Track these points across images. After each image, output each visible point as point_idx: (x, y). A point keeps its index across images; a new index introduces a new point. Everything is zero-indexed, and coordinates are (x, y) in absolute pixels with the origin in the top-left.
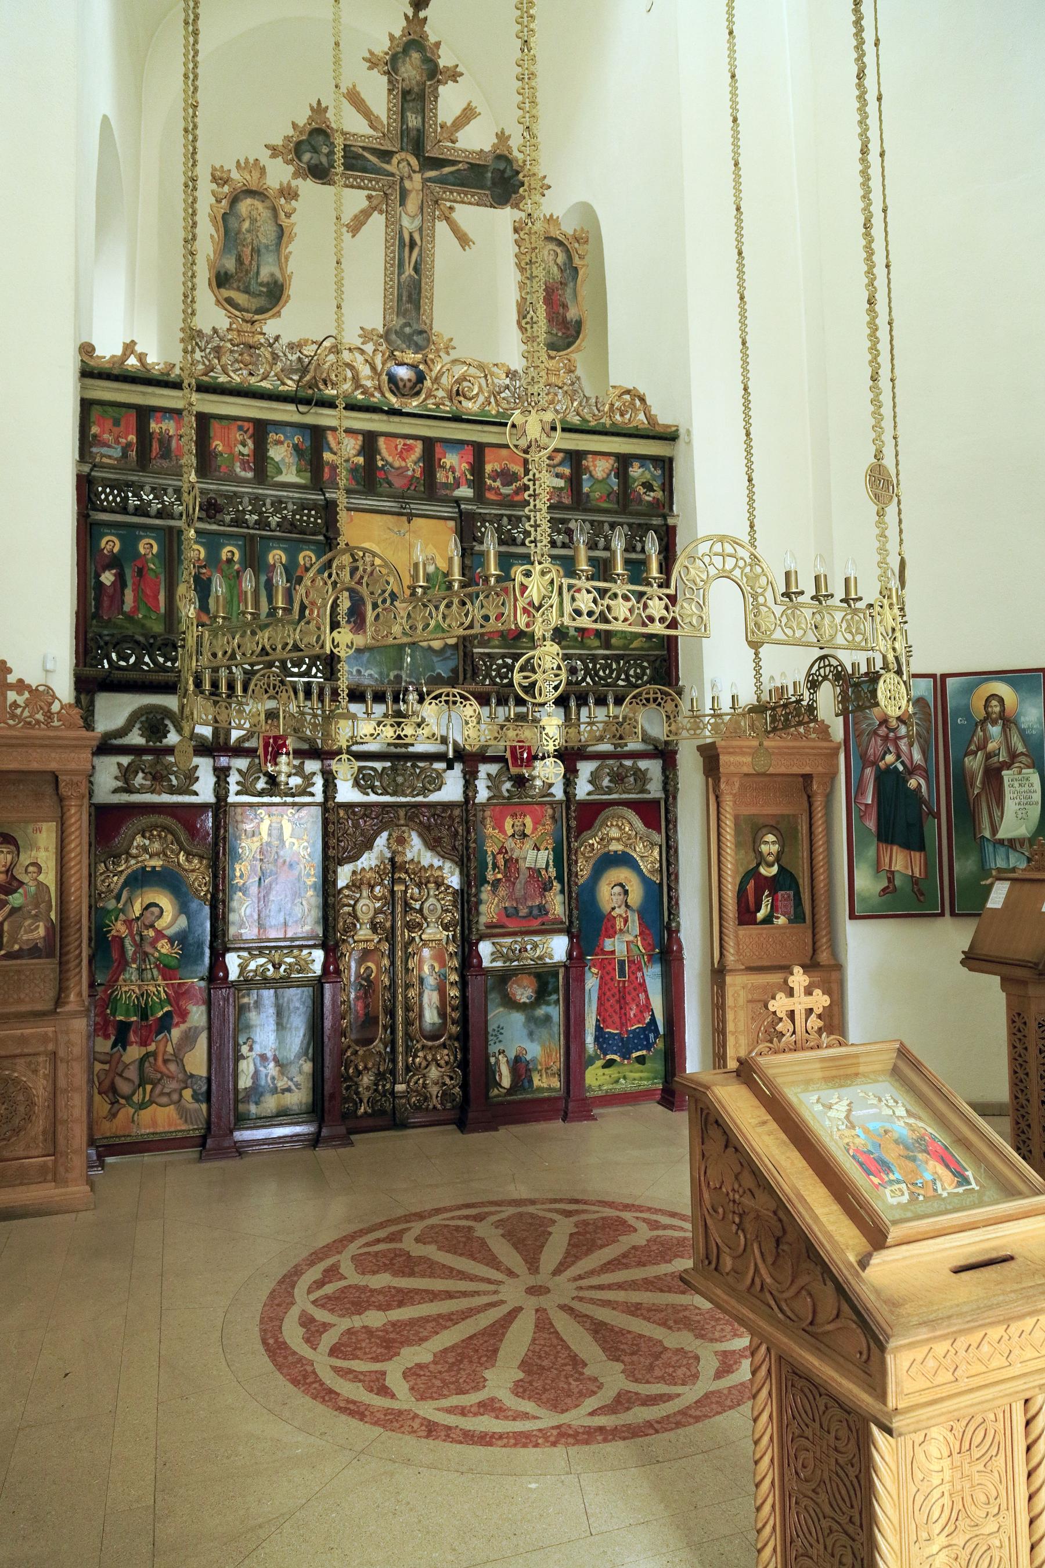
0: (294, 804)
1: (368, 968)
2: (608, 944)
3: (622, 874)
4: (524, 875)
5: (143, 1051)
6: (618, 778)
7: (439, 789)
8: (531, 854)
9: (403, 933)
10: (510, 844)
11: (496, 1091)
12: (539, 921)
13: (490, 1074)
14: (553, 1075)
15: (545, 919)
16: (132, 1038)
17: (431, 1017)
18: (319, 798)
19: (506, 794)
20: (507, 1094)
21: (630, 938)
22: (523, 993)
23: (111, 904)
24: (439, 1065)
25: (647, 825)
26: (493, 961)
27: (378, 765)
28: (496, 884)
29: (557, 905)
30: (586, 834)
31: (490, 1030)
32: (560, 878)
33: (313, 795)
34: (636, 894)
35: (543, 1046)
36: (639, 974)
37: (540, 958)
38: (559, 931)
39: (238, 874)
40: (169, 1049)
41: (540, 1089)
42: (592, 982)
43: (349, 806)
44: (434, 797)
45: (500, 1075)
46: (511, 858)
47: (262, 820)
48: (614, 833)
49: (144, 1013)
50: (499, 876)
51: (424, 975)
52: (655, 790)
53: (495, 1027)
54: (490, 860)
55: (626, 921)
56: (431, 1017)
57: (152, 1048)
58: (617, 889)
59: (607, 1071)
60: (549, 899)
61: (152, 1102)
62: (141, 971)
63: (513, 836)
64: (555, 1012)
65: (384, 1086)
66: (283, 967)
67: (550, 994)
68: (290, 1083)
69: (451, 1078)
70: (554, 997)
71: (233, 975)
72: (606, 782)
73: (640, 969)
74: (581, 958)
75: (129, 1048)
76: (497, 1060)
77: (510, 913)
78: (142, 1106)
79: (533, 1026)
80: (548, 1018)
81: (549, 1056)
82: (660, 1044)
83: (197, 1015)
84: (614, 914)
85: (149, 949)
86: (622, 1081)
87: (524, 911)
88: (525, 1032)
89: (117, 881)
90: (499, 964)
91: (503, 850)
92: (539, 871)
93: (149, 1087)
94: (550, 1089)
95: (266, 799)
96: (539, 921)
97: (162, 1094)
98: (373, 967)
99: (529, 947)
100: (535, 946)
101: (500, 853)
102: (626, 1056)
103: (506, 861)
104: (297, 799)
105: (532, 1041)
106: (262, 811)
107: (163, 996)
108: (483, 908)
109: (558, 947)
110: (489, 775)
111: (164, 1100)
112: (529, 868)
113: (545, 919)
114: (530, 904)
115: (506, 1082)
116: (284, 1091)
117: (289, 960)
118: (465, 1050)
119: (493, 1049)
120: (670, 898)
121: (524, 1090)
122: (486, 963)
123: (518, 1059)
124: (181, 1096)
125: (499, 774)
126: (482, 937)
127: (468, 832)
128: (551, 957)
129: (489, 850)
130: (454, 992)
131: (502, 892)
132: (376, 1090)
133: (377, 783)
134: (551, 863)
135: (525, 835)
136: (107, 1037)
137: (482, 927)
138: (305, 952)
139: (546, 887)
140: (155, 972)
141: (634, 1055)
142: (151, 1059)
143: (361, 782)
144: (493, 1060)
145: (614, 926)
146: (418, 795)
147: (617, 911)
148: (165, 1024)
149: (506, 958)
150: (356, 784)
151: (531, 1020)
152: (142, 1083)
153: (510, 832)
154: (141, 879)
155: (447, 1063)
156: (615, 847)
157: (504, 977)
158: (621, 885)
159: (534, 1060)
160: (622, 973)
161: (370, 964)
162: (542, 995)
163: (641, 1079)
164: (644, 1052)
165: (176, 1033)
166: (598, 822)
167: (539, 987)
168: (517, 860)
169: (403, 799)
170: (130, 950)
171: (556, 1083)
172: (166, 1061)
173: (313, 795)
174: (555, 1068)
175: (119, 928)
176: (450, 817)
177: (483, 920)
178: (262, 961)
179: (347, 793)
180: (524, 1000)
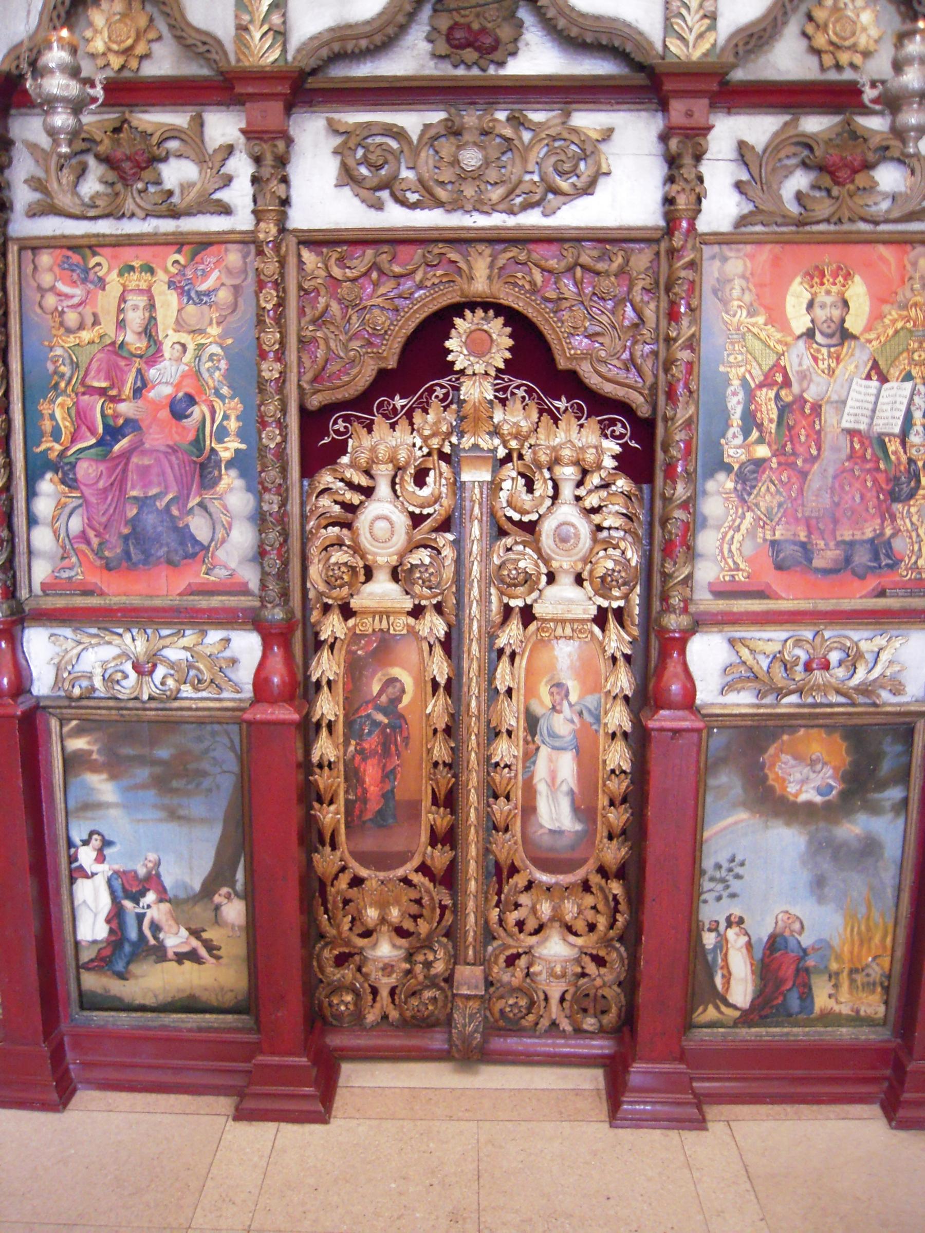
0: (178, 242)
1: (393, 681)
4: (834, 453)
7: (588, 189)
8: (862, 391)
9: (485, 599)
10: (797, 358)
11: (711, 1013)
12: (872, 583)
13: (696, 975)
14: (870, 987)
15: (888, 580)
17: (555, 814)
18: (243, 220)
19: (793, 208)
20: (736, 1023)
22: (807, 777)
24: (570, 929)
26: (727, 688)
27: (412, 121)
28: (749, 475)
31: (708, 863)
33: (225, 210)
35: (851, 917)
37: (865, 689)
39: (47, 425)
41: (828, 1018)
43: (318, 241)
44: (575, 215)
45: (727, 978)
46: (801, 400)
47: (102, 283)
50: (762, 451)
51: (538, 709)
53: (723, 858)
54: (735, 405)
56: (555, 814)
63: (810, 334)
65: (428, 965)
66: (160, 671)
67: (882, 786)
68: (195, 943)
69: (600, 961)
70: (895, 794)
76: (722, 944)
77: (789, 559)
79: (826, 866)
80: (870, 848)
81: (865, 940)
87: (826, 555)
88: (804, 877)
90: (743, 700)
91: (777, 377)
92: (881, 441)
94: (857, 1020)
95: (105, 227)
96: (872, 583)
98: (407, 680)
99: (834, 657)
100: (852, 659)
101: (767, 382)
103: (784, 410)
104: (189, 225)
105: (821, 900)
106: (101, 262)
108: (707, 541)
110: (742, 147)
112: (852, 433)
113: (888, 580)
114: (846, 534)
115: (741, 991)
116: (180, 958)
117: (174, 654)
118: (636, 899)
119: (711, 911)
121: (785, 1016)
122: (707, 693)
123: (775, 943)
125: (776, 145)
126: (698, 624)
127: (673, 316)
128: (898, 689)
129: (735, 374)
130: (618, 756)
131: (767, 496)
132: (409, 972)
133: (406, 174)
135: (845, 335)
138: (214, 636)
143: (367, 170)
144: (709, 939)
146: (527, 206)
150: (348, 177)
151: (821, 847)
153: (800, 322)
155: (592, 927)
157: (756, 736)
159: (823, 946)
161: (396, 672)
162: (858, 786)
167: (855, 764)
168: (817, 408)
169: (480, 221)
171: (873, 1005)
173: (225, 210)
174: (876, 972)
176: (622, 272)
177: (707, 572)
178: (107, 652)
179: (321, 198)
180: (809, 795)
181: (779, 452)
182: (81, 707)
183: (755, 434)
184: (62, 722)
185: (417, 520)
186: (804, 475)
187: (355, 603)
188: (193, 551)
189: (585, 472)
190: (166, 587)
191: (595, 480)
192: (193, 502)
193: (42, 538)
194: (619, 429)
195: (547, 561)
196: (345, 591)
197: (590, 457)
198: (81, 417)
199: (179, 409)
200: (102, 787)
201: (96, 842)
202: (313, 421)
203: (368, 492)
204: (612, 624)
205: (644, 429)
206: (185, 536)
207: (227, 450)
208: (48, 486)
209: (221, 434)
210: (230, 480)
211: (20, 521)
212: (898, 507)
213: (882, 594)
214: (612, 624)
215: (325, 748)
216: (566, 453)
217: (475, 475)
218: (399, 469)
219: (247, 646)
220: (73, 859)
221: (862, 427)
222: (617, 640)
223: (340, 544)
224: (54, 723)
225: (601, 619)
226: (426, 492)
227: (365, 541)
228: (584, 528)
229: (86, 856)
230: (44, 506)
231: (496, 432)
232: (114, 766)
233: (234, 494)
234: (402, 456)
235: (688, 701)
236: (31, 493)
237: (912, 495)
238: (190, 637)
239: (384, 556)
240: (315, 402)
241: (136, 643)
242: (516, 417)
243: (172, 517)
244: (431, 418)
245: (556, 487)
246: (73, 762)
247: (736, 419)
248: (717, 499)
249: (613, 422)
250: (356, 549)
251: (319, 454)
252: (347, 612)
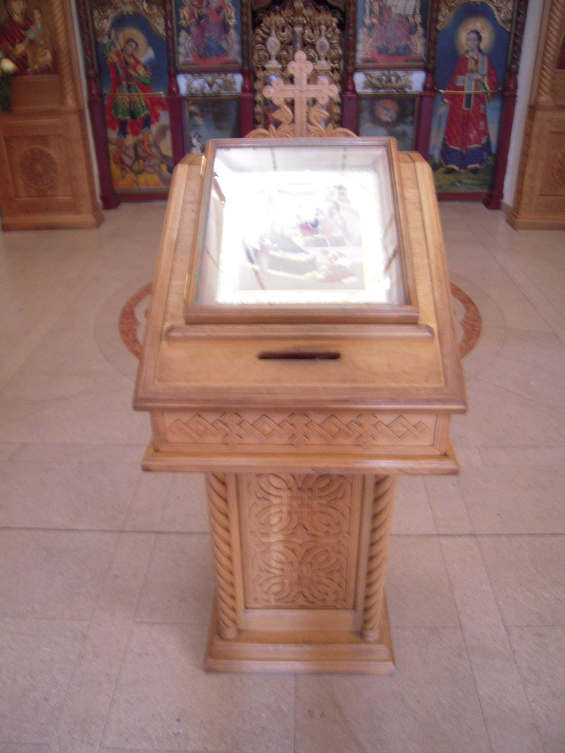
3: (478, 24)
5: (136, 139)
16: (129, 130)
21: (478, 77)
23: (106, 40)
28: (371, 27)
29: (419, 47)
32: (423, 24)
36: (482, 106)
37: (402, 88)
38: (418, 68)
39: (182, 16)
40: (151, 139)
42: (442, 110)
46: (385, 5)
49: (133, 114)
50: (374, 20)
55: (477, 62)
57: (140, 136)
58: (473, 36)
59: (447, 176)
60: (413, 41)
61: (144, 171)
62: (129, 87)
64: (409, 130)
66: (215, 86)
70: (410, 119)
71: (183, 90)
73: (483, 102)
74: (433, 90)
75: (127, 136)
77: (383, 51)
78: (138, 173)
82: (490, 160)
83: (164, 118)
84: (468, 57)
85: (131, 72)
86: (458, 184)
87: (393, 49)
89: (107, 24)
90: (369, 91)
93: (141, 161)
97: (150, 166)
99: (393, 79)
102: (463, 166)
103: (381, 8)
107: (144, 103)
109: (417, 80)
111: (150, 170)
112: (399, 15)
114: (397, 44)
117: (219, 81)
120: (515, 44)
122: (359, 89)
124: (160, 168)
128: (410, 88)
134: (418, 11)
136: (114, 129)
137: (359, 62)
138: (229, 76)
139: (412, 31)
140: (137, 86)
141: (471, 166)
142: (141, 144)
145: (466, 67)
147: (471, 54)
148: (147, 123)
149: (374, 87)
152: (137, 157)
154: (121, 22)
160: (468, 105)
162: (401, 118)
163: (473, 185)
164: (477, 166)
165: (154, 129)
168: (390, 8)
170: (121, 72)
172: (149, 146)
175: (113, 58)
181: (379, 20)
182: (193, 97)
183: (372, 15)
184: (188, 101)
185: (282, 43)
186: (385, 27)
187: (266, 66)
188: (225, 52)
189: (327, 27)
190: (214, 63)
191: (330, 29)
192: (223, 37)
193: (181, 50)
194: (338, 14)
195: (317, 53)
196: (263, 63)
197: (329, 22)
198: (192, 14)
199: (218, 11)
200: (199, 121)
201: (197, 136)
202: (254, 14)
203: (269, 35)
204: (335, 72)
205: (344, 14)
206: (220, 47)
207: (232, 22)
208: (183, 34)
209: (230, 18)
210: (232, 32)
211: (176, 44)
212: (411, 36)
213: (406, 61)
214: (335, 72)
215: (258, 109)
216: (322, 21)
217: (298, 29)
218: (277, 27)
219: (239, 79)
220: (191, 141)
221: (402, 12)
222: (336, 77)
223: (262, 49)
224: (186, 102)
225: (333, 70)
226: (284, 34)
227: (269, 48)
228: (327, 43)
229: (194, 141)
230: (182, 40)
231: (303, 16)
232: (203, 115)
233: (233, 34)
234: (278, 23)
235: (354, 91)
236: (178, 36)
237: (415, 32)
238: (223, 76)
239: (273, 53)
240: (255, 8)
241: (209, 78)
242: (308, 12)
243: (217, 42)
244: (286, 11)
245: (320, 32)
246: (192, 114)
247: (368, 12)
248: (362, 34)
249: (336, 12)
250: (267, 51)
251: (257, 24)
252: (264, 69)
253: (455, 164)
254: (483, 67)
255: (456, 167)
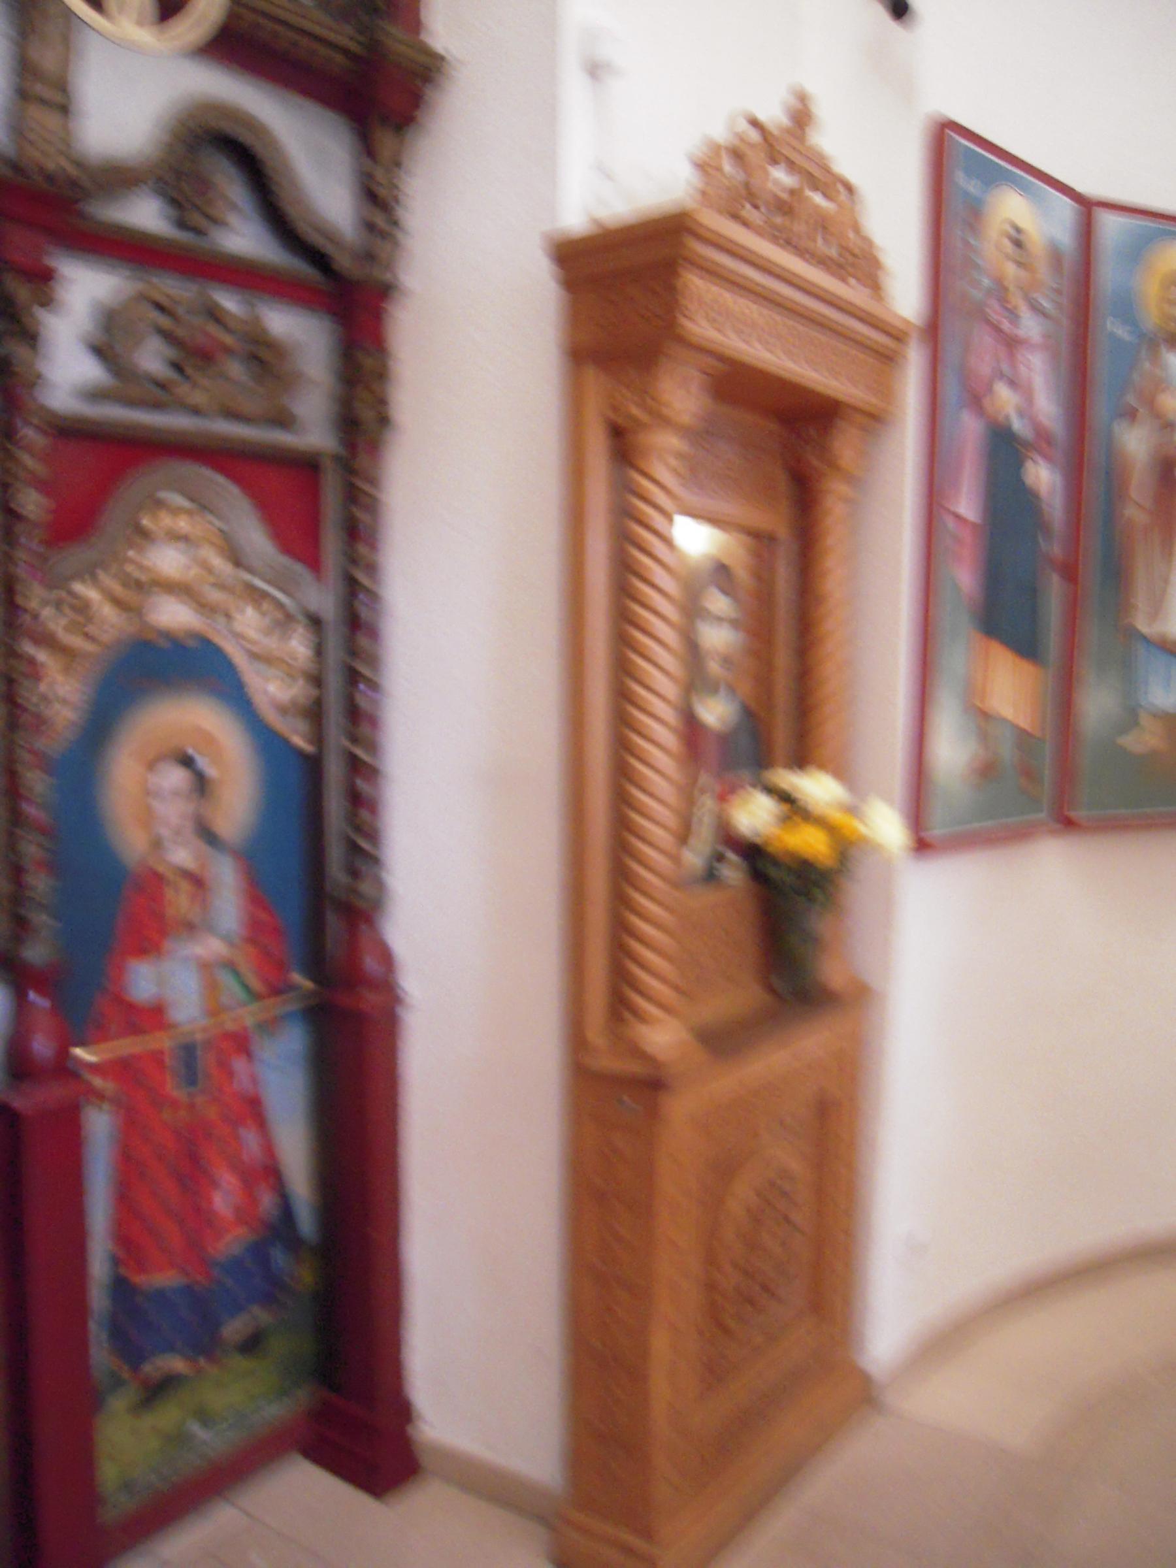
2: (144, 981)
6: (194, 356)
25: (286, 546)
30: (75, 556)
34: (239, 801)
48: (168, 560)
52: (313, 429)
58: (174, 777)
72: (152, 358)
156: (173, 615)
158: (187, 762)
166: (114, 514)
253: (170, 1348)
254: (229, 905)
255: (177, 1364)
